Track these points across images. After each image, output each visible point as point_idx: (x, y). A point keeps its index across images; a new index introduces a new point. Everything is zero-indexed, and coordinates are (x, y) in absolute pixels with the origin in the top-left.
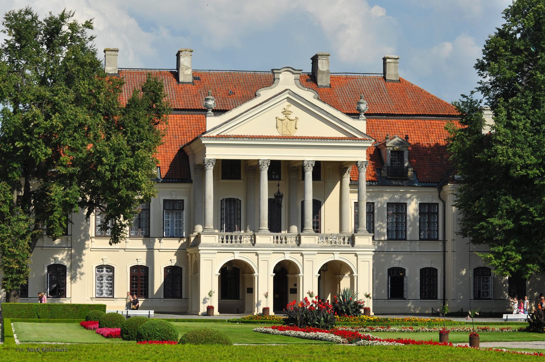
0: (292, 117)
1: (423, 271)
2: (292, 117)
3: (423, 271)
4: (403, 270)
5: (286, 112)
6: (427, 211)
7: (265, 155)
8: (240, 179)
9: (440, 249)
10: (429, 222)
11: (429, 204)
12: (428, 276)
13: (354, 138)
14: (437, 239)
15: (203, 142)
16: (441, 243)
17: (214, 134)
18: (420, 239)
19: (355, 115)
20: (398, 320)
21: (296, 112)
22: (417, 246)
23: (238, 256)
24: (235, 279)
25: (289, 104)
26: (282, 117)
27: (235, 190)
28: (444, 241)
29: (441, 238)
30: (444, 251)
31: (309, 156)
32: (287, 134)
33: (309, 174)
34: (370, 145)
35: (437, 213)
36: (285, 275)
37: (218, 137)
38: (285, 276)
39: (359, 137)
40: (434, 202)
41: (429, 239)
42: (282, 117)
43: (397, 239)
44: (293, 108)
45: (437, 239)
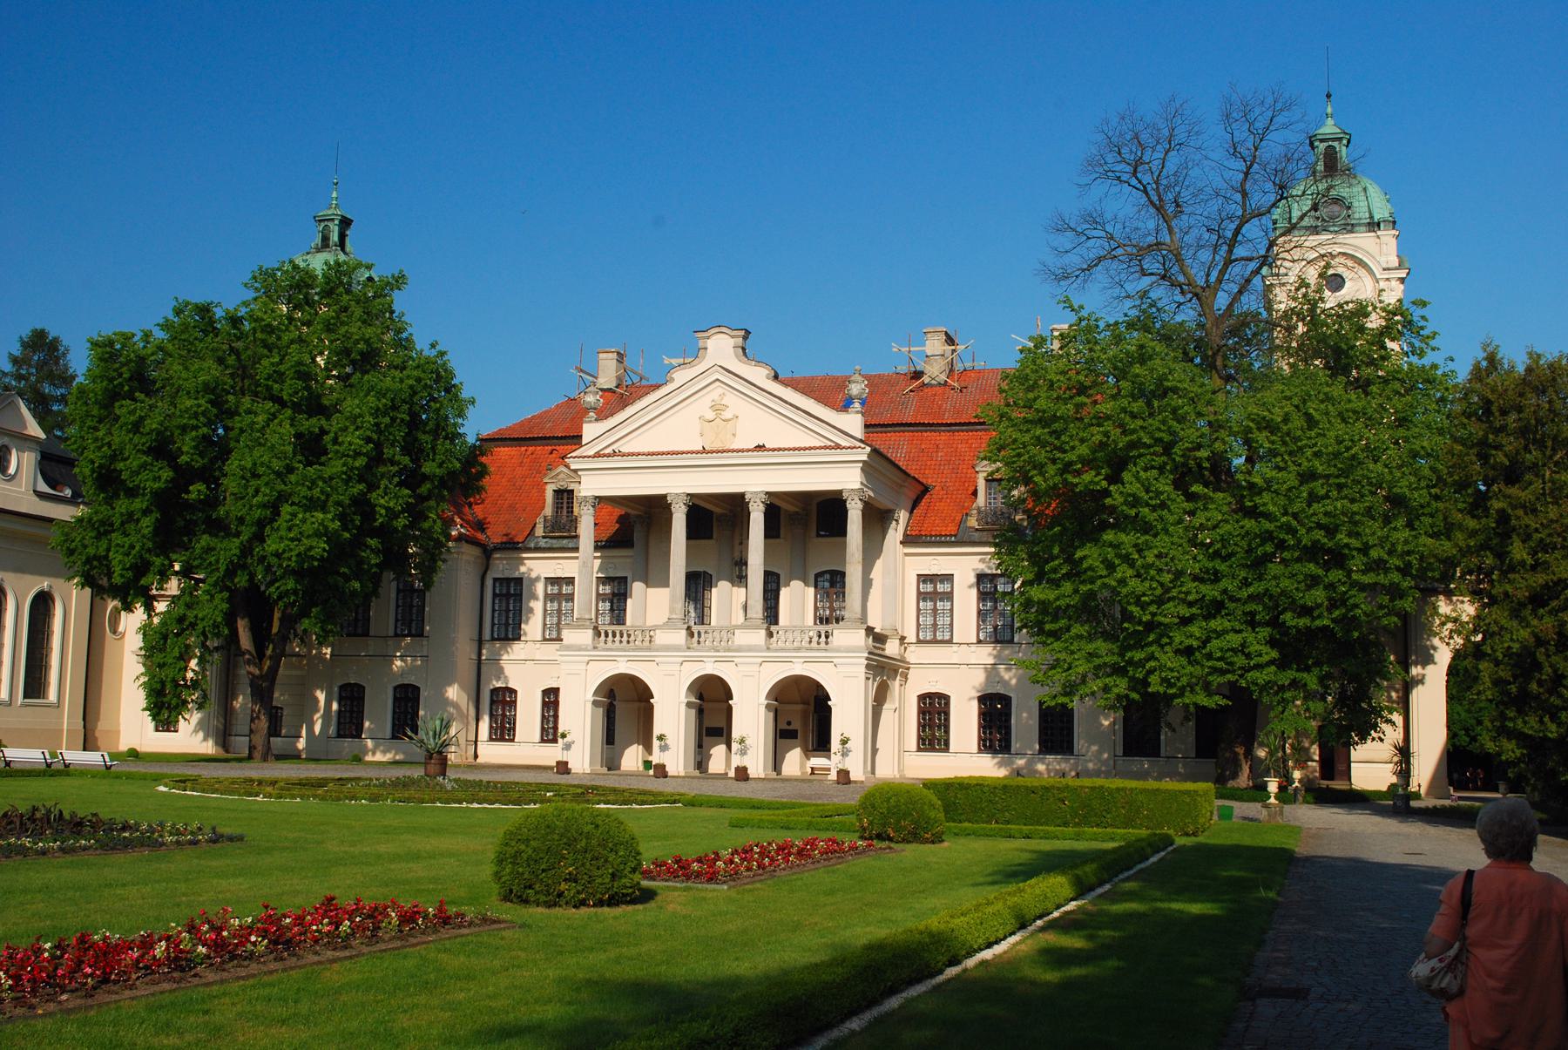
0: (727, 415)
2: (727, 415)
5: (718, 408)
7: (678, 485)
8: (710, 537)
13: (838, 447)
15: (573, 467)
17: (592, 453)
19: (845, 406)
21: (735, 404)
25: (720, 391)
26: (710, 415)
31: (757, 483)
32: (717, 445)
34: (865, 458)
37: (598, 455)
39: (844, 444)
42: (710, 415)
44: (731, 399)
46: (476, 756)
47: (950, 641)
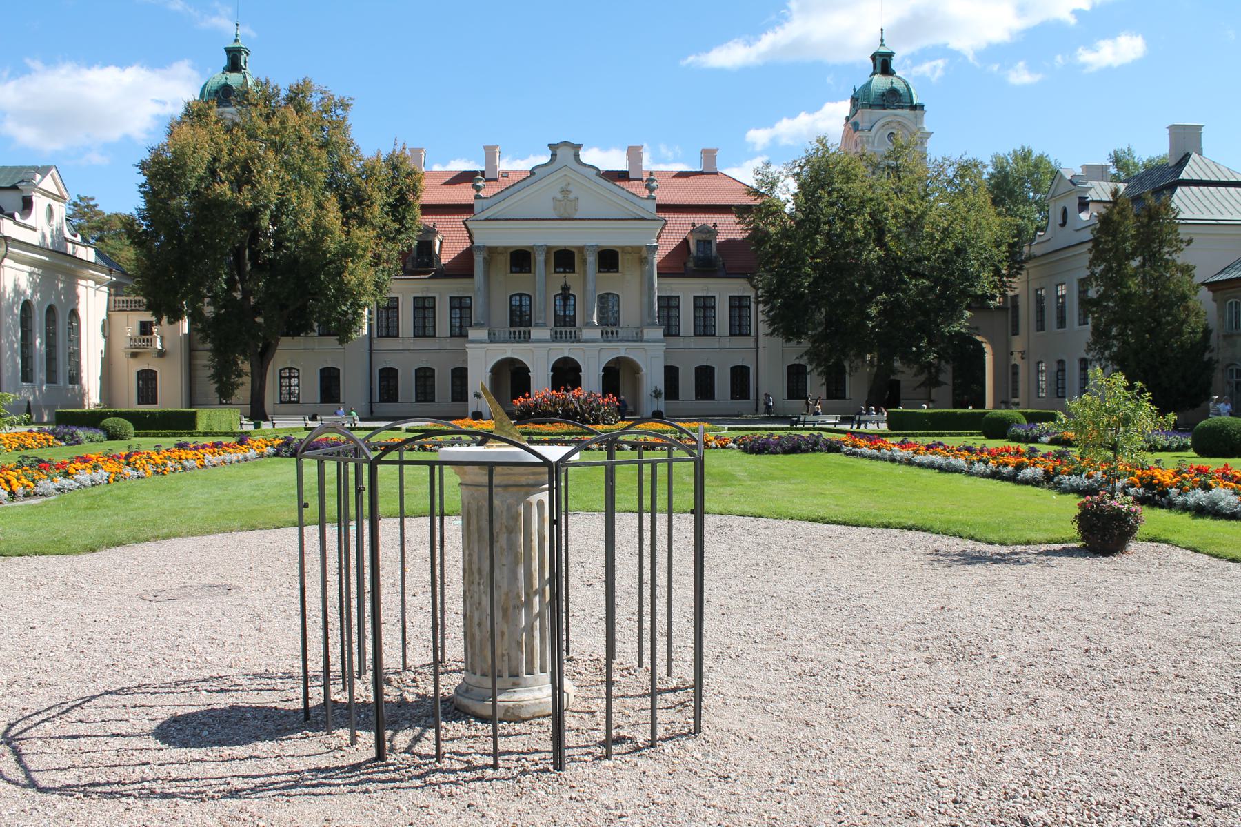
0: (572, 196)
1: (734, 369)
2: (572, 196)
3: (734, 369)
4: (712, 369)
5: (565, 192)
6: (738, 305)
9: (753, 345)
10: (740, 317)
11: (740, 297)
12: (740, 376)
14: (749, 335)
16: (753, 339)
18: (731, 335)
20: (460, 445)
22: (728, 342)
23: (509, 355)
24: (512, 377)
26: (560, 196)
27: (520, 283)
28: (757, 336)
29: (753, 333)
30: (757, 348)
32: (566, 216)
33: (592, 260)
35: (749, 307)
36: (566, 374)
37: (486, 220)
38: (566, 374)
40: (746, 294)
41: (741, 335)
42: (560, 196)
43: (705, 335)
45: (749, 335)
46: (372, 412)
47: (678, 335)
